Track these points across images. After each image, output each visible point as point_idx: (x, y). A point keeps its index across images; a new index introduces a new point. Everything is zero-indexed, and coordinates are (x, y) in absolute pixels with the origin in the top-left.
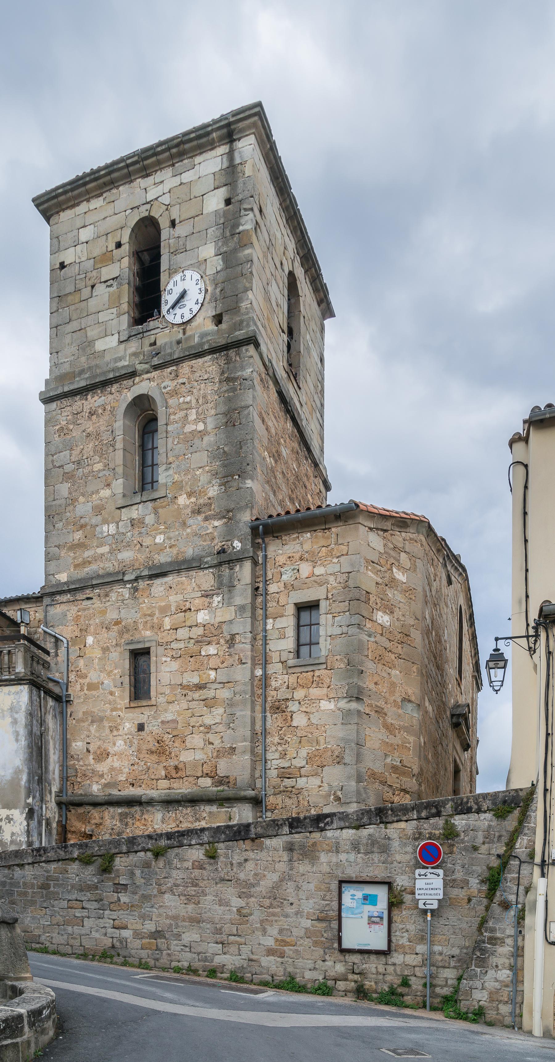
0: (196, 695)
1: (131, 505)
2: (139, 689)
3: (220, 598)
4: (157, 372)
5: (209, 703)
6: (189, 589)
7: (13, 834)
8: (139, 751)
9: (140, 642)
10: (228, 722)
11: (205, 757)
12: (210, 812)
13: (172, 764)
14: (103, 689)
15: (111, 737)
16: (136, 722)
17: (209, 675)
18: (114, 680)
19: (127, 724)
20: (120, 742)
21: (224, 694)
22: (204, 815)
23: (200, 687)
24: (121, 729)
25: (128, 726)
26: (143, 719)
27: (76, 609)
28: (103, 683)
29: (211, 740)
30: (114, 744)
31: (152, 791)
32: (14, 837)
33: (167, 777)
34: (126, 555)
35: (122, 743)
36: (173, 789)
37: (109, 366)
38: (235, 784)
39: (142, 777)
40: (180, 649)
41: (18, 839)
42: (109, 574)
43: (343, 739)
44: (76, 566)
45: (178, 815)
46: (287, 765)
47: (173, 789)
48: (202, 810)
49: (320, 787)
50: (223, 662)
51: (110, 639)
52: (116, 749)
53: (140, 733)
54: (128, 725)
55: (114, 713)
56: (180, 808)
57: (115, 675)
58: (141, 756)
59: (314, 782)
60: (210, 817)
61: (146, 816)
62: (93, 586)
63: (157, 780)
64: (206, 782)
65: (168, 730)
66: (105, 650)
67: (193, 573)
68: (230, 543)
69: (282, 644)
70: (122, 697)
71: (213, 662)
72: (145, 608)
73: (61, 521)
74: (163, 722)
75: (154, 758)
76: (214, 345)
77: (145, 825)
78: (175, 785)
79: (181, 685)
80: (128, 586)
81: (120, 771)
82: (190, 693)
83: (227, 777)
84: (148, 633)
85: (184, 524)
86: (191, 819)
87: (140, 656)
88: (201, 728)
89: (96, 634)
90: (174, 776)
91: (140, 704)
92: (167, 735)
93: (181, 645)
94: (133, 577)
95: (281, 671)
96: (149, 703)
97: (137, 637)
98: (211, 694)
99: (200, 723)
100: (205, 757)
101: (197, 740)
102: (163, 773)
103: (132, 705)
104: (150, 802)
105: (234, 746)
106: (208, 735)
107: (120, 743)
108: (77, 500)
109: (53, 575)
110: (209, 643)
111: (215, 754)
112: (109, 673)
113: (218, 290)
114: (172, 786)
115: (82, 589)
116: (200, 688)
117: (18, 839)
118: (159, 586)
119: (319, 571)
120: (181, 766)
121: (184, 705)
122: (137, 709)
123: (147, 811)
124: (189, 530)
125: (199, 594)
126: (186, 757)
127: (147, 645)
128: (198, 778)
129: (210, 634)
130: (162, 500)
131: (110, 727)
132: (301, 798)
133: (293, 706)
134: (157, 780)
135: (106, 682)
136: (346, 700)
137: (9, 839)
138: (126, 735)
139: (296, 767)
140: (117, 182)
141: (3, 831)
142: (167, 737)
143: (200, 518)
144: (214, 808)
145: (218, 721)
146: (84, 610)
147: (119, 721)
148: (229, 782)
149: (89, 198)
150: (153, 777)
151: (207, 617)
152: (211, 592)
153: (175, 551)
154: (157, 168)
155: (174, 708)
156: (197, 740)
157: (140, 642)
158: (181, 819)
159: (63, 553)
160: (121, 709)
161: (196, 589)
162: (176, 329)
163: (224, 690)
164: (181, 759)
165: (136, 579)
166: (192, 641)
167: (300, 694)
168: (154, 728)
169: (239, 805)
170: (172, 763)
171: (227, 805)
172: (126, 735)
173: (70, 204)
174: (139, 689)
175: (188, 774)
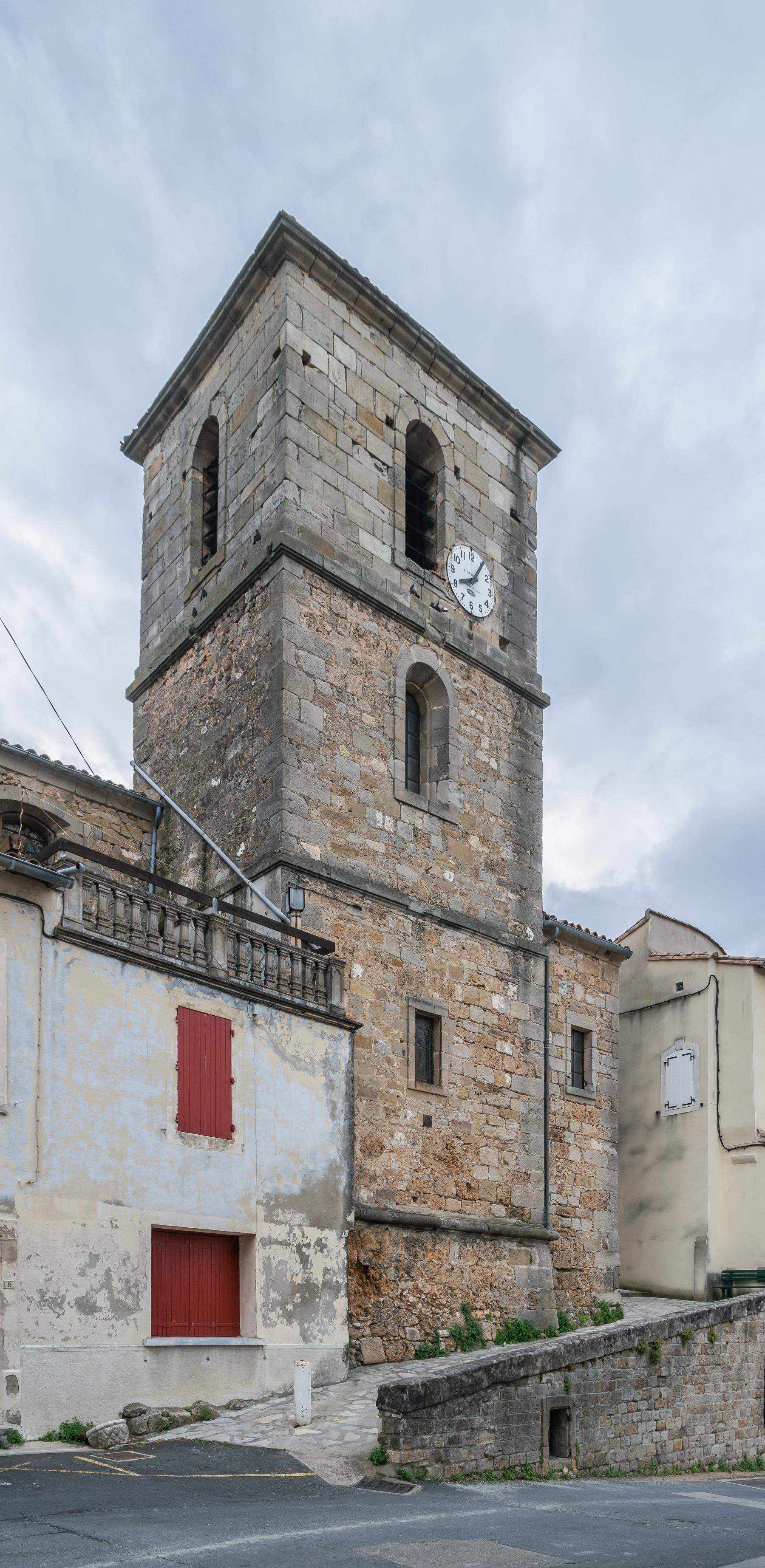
0: (492, 1098)
1: (416, 808)
2: (428, 1070)
3: (515, 989)
4: (445, 652)
5: (505, 1113)
6: (484, 961)
7: (326, 1271)
8: (424, 1152)
9: (429, 1004)
10: (523, 1141)
11: (500, 1179)
12: (510, 1250)
13: (464, 1179)
14: (376, 1051)
15: (387, 1124)
16: (422, 1113)
17: (504, 1078)
18: (392, 1042)
19: (409, 1112)
20: (400, 1134)
21: (519, 1106)
22: (505, 1253)
23: (494, 1089)
24: (402, 1117)
25: (411, 1115)
26: (431, 1110)
27: (338, 912)
28: (376, 1042)
29: (506, 1160)
30: (392, 1136)
31: (441, 1212)
32: (328, 1276)
33: (459, 1197)
34: (409, 874)
35: (403, 1137)
36: (465, 1213)
37: (384, 587)
38: (529, 1218)
39: (428, 1191)
40: (474, 1033)
41: (334, 1280)
42: (382, 886)
43: (608, 1184)
44: (335, 847)
45: (477, 1250)
46: (564, 1202)
47: (465, 1213)
48: (502, 1246)
49: (592, 1231)
50: (517, 1068)
51: (386, 982)
52: (394, 1143)
53: (426, 1128)
54: (410, 1113)
55: (392, 1091)
56: (478, 1241)
57: (394, 1036)
58: (428, 1161)
59: (586, 1225)
60: (511, 1257)
61: (439, 1247)
62: (365, 893)
63: (446, 1197)
64: (500, 1210)
65: (459, 1134)
66: (380, 994)
67: (487, 942)
68: (523, 927)
69: (562, 1066)
70: (404, 1073)
71: (509, 1064)
72: (433, 960)
73: (312, 761)
74: (454, 1122)
75: (442, 1166)
76: (513, 679)
77: (439, 1259)
78: (468, 1209)
79: (474, 1079)
80: (410, 917)
81: (400, 1177)
82: (484, 1093)
83: (522, 1208)
84: (436, 995)
85: (476, 874)
86: (492, 1257)
87: (429, 1023)
88: (496, 1142)
89: (366, 965)
90: (467, 1197)
91: (429, 1090)
92: (456, 1140)
93: (476, 1030)
94: (420, 910)
95: (559, 1095)
96: (439, 1092)
97: (423, 995)
98: (506, 1101)
99: (495, 1134)
100: (500, 1179)
101: (490, 1155)
102: (454, 1190)
103: (419, 1088)
104: (446, 1230)
105: (529, 1172)
106: (504, 1153)
107: (399, 1135)
108: (337, 746)
109: (298, 839)
110: (504, 1039)
111: (510, 1178)
112: (386, 1031)
113: (506, 610)
114: (463, 1209)
115: (348, 888)
116: (495, 1091)
117: (334, 1280)
118: (450, 938)
119: (590, 999)
120: (474, 1185)
121: (478, 1107)
122: (423, 1096)
123: (441, 1240)
124: (481, 885)
125: (494, 973)
126: (480, 1174)
127: (438, 1012)
128: (491, 1203)
129: (503, 1028)
130: (452, 827)
131: (386, 1109)
132: (577, 1241)
133: (569, 1138)
134: (446, 1197)
135: (381, 1041)
136: (610, 1144)
137: (321, 1279)
138: (408, 1126)
139: (571, 1206)
140: (394, 335)
141: (312, 1265)
142: (458, 1143)
143: (493, 878)
144: (514, 1246)
145: (513, 1138)
146: (349, 920)
147: (398, 1104)
148: (522, 1215)
149: (353, 308)
150: (441, 1193)
151: (503, 1006)
152: (506, 977)
153: (466, 902)
154: (443, 381)
155: (466, 1106)
156: (490, 1155)
157: (429, 1004)
158: (481, 1255)
159: (315, 813)
160: (401, 1088)
161: (491, 964)
162: (461, 612)
163: (519, 1102)
164: (474, 1176)
165: (423, 915)
166: (488, 1029)
167: (575, 1126)
168: (444, 1127)
169: (539, 1245)
170: (464, 1178)
171: (526, 1243)
172: (408, 1126)
173: (325, 282)
174: (428, 1070)
175: (482, 1196)
